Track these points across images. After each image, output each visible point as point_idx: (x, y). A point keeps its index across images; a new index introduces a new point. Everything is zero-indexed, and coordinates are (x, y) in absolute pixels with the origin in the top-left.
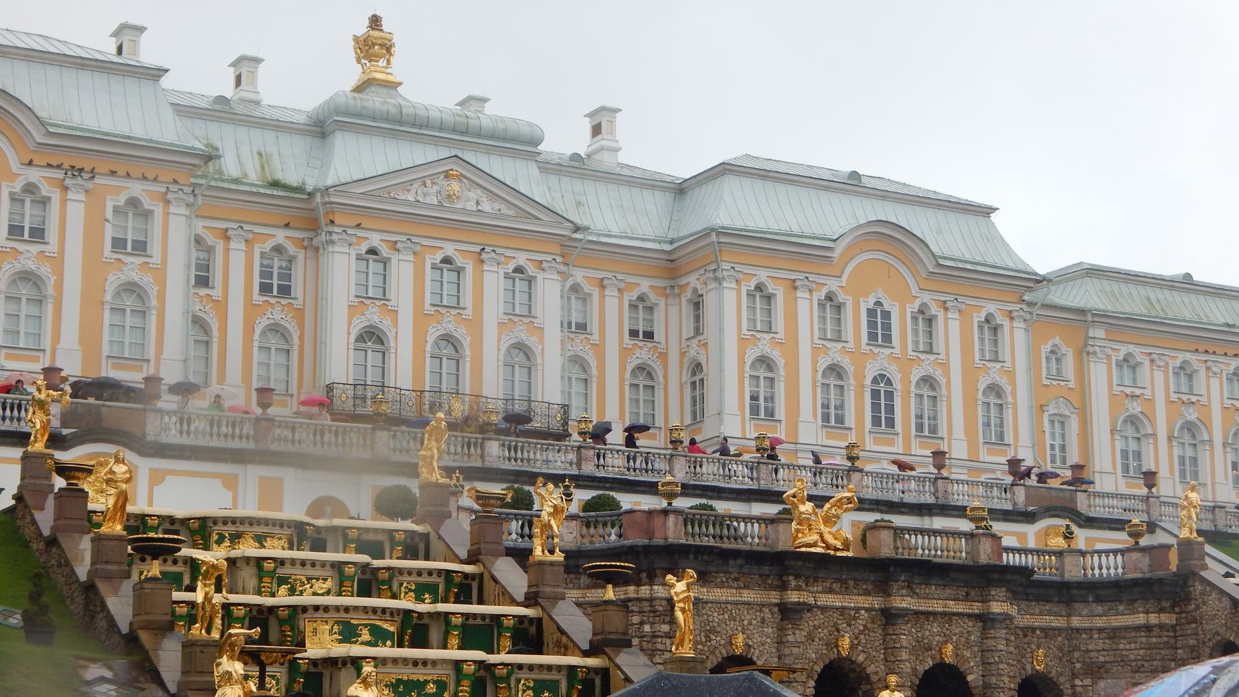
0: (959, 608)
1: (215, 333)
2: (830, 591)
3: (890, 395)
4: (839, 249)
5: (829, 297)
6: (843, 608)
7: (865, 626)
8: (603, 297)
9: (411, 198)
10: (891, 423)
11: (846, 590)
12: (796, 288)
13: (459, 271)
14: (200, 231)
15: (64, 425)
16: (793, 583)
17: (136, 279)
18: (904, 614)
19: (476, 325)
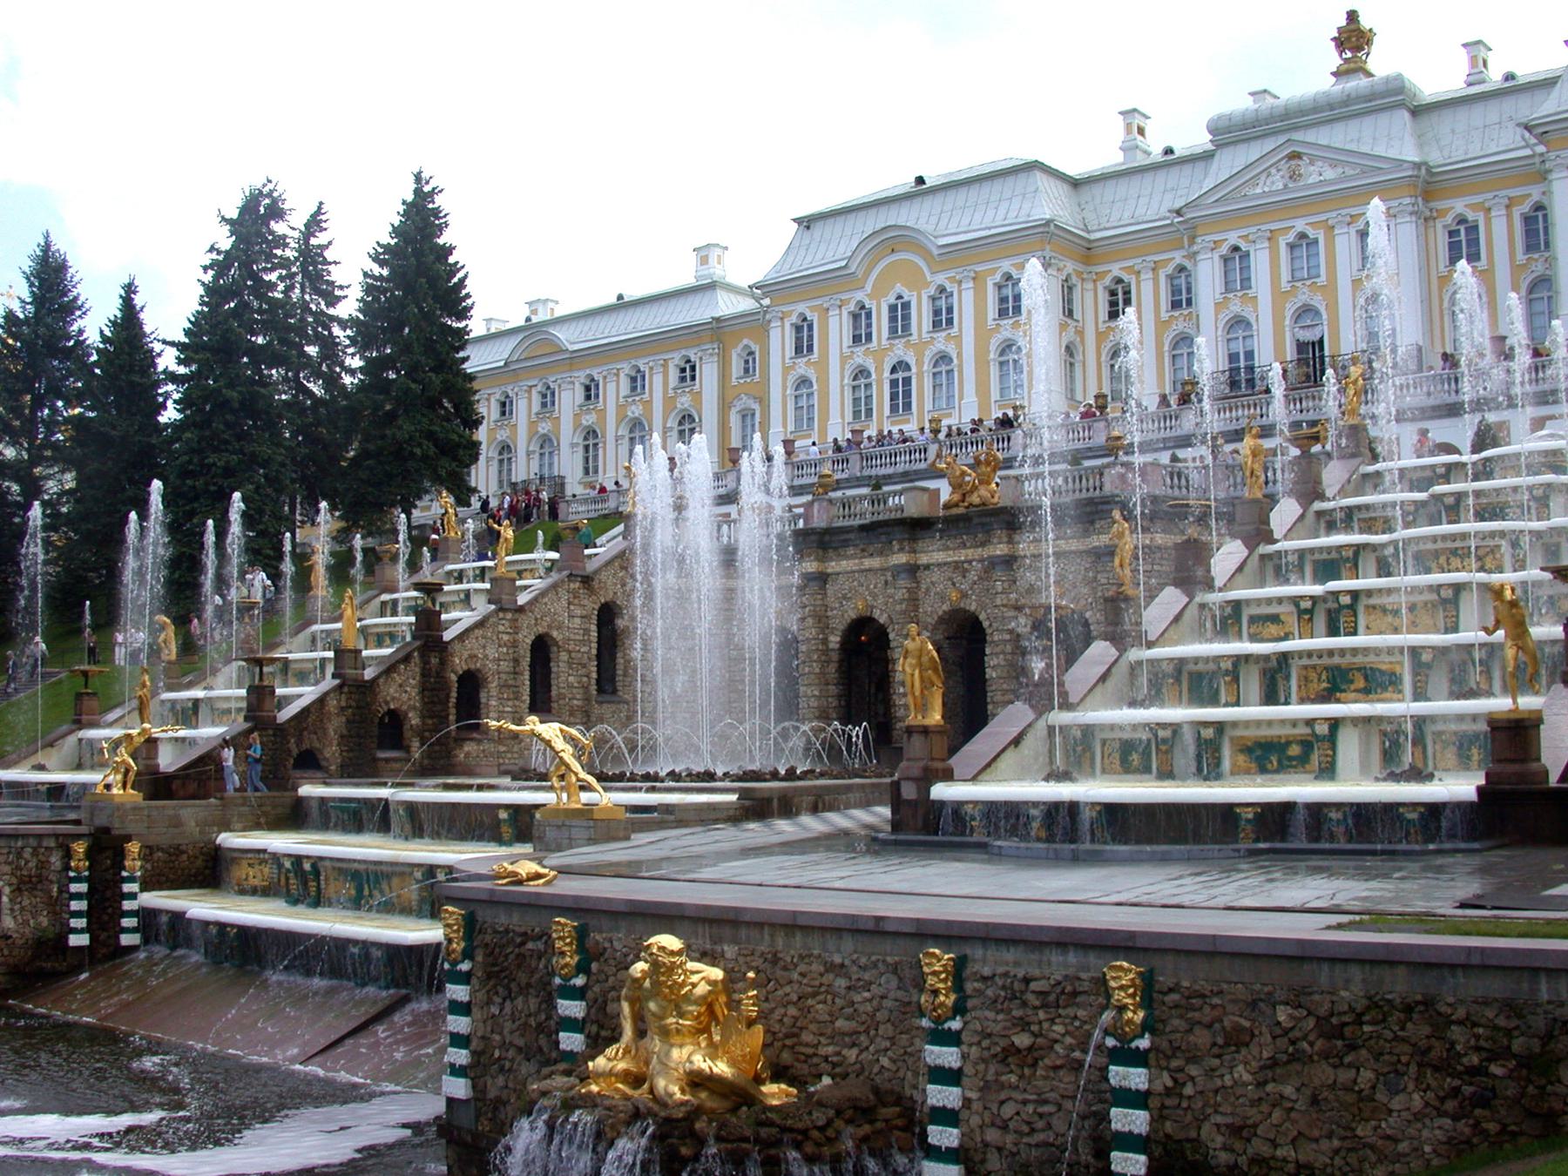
6: (956, 562)
7: (980, 578)
9: (1258, 190)
11: (964, 546)
13: (1316, 241)
17: (1010, 336)
18: (1010, 561)
19: (1330, 289)
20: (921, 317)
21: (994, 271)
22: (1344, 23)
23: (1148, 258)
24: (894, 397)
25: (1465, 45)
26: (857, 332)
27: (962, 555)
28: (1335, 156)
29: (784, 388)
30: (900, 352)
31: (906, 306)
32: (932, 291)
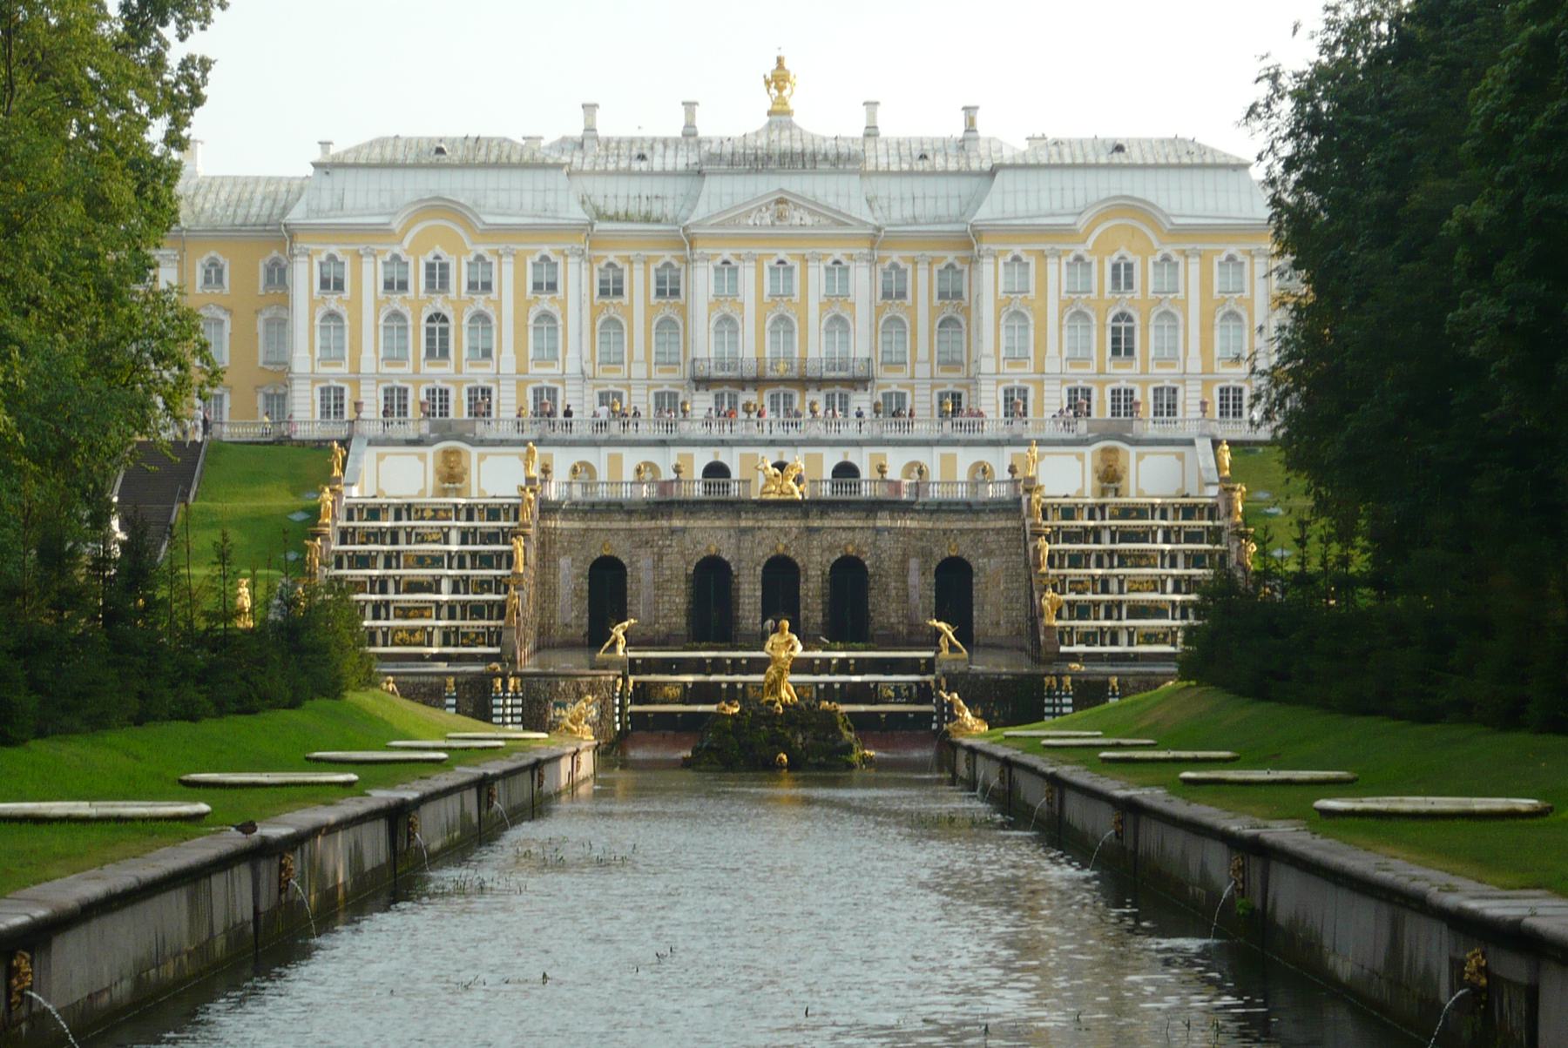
0: (860, 524)
1: (625, 327)
2: (774, 519)
3: (1130, 331)
4: (1081, 224)
5: (1079, 259)
8: (915, 271)
9: (751, 222)
10: (1130, 352)
11: (785, 518)
12: (1046, 257)
13: (791, 269)
14: (611, 259)
15: (431, 432)
16: (743, 515)
18: (818, 530)
20: (459, 277)
21: (533, 252)
22: (774, 65)
23: (642, 253)
24: (430, 342)
25: (865, 104)
26: (389, 277)
27: (786, 524)
28: (815, 208)
29: (312, 319)
30: (439, 305)
31: (444, 267)
32: (471, 258)
